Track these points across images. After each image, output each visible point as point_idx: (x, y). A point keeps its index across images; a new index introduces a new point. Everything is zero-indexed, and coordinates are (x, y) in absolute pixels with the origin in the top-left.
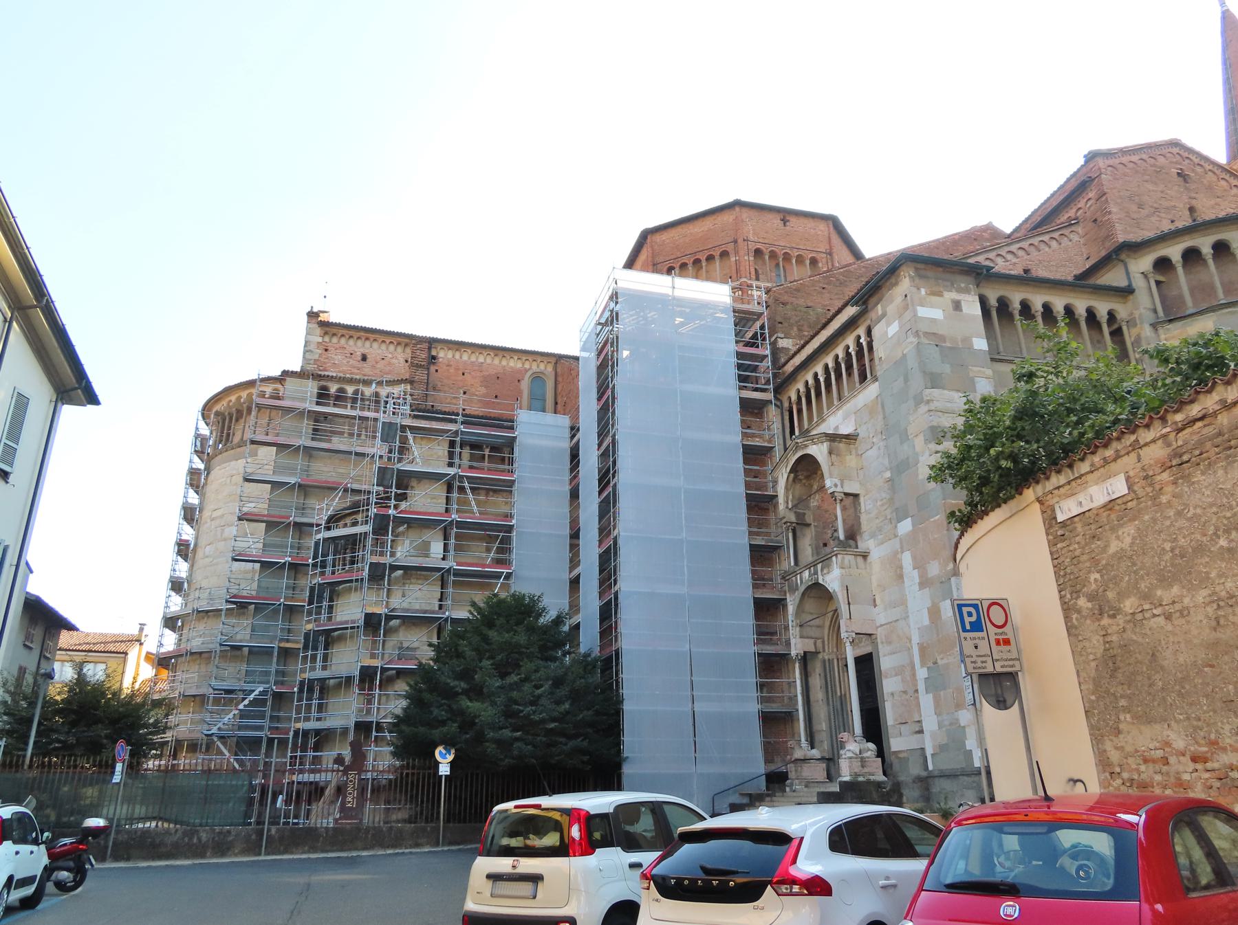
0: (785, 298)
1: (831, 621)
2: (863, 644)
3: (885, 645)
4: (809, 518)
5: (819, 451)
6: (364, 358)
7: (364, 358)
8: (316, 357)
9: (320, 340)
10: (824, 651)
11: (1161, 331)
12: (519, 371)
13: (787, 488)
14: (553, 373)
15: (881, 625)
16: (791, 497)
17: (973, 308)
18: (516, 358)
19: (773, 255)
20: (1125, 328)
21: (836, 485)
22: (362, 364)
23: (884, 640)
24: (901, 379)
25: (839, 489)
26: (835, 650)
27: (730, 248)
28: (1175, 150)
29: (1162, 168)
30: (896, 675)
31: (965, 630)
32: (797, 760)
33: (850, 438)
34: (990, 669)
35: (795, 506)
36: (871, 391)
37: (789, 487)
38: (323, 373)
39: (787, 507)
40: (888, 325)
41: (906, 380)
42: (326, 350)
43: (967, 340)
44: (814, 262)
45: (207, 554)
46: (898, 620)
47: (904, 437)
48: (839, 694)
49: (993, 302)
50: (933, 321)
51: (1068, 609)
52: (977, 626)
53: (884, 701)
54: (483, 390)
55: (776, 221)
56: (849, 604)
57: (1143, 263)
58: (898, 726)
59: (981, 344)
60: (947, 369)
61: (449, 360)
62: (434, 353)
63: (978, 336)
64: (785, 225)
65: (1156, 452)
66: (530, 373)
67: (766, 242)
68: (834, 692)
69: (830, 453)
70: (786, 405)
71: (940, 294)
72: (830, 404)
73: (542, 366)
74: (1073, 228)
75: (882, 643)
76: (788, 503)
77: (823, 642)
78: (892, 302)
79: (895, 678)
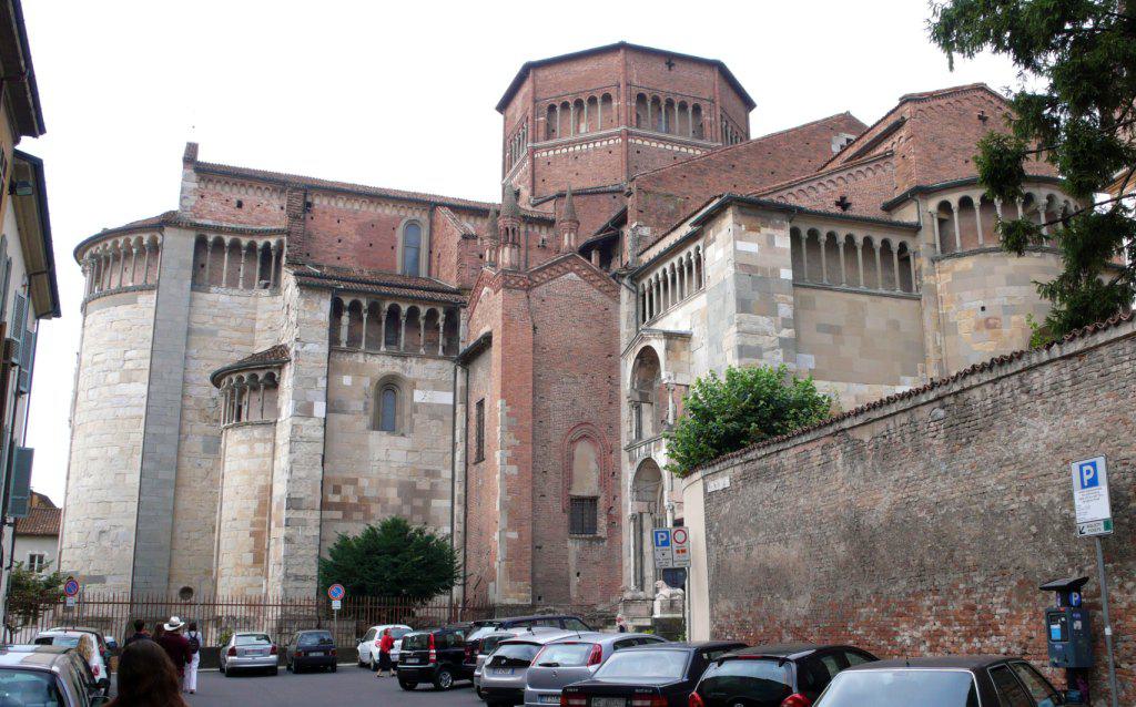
0: (648, 186)
5: (659, 346)
6: (240, 205)
7: (240, 205)
8: (193, 203)
9: (196, 185)
11: (936, 265)
12: (395, 218)
13: (633, 372)
14: (428, 221)
17: (783, 241)
18: (391, 205)
19: (656, 101)
20: (912, 258)
21: (669, 378)
22: (237, 211)
24: (722, 299)
25: (672, 381)
27: (613, 92)
28: (981, 93)
29: (965, 111)
31: (657, 545)
33: (685, 337)
34: (670, 566)
35: (640, 387)
36: (699, 302)
38: (198, 221)
40: (716, 249)
41: (725, 302)
42: (202, 197)
43: (776, 271)
44: (697, 109)
45: (91, 398)
47: (720, 349)
49: (804, 234)
50: (749, 254)
51: (708, 539)
52: (666, 543)
54: (358, 238)
55: (661, 66)
57: (932, 205)
59: (787, 274)
60: (756, 296)
61: (325, 207)
62: (309, 199)
63: (786, 267)
64: (670, 69)
65: (738, 470)
66: (405, 221)
67: (650, 86)
69: (667, 349)
70: (641, 291)
71: (757, 230)
72: (674, 302)
73: (417, 215)
74: (888, 160)
78: (721, 230)
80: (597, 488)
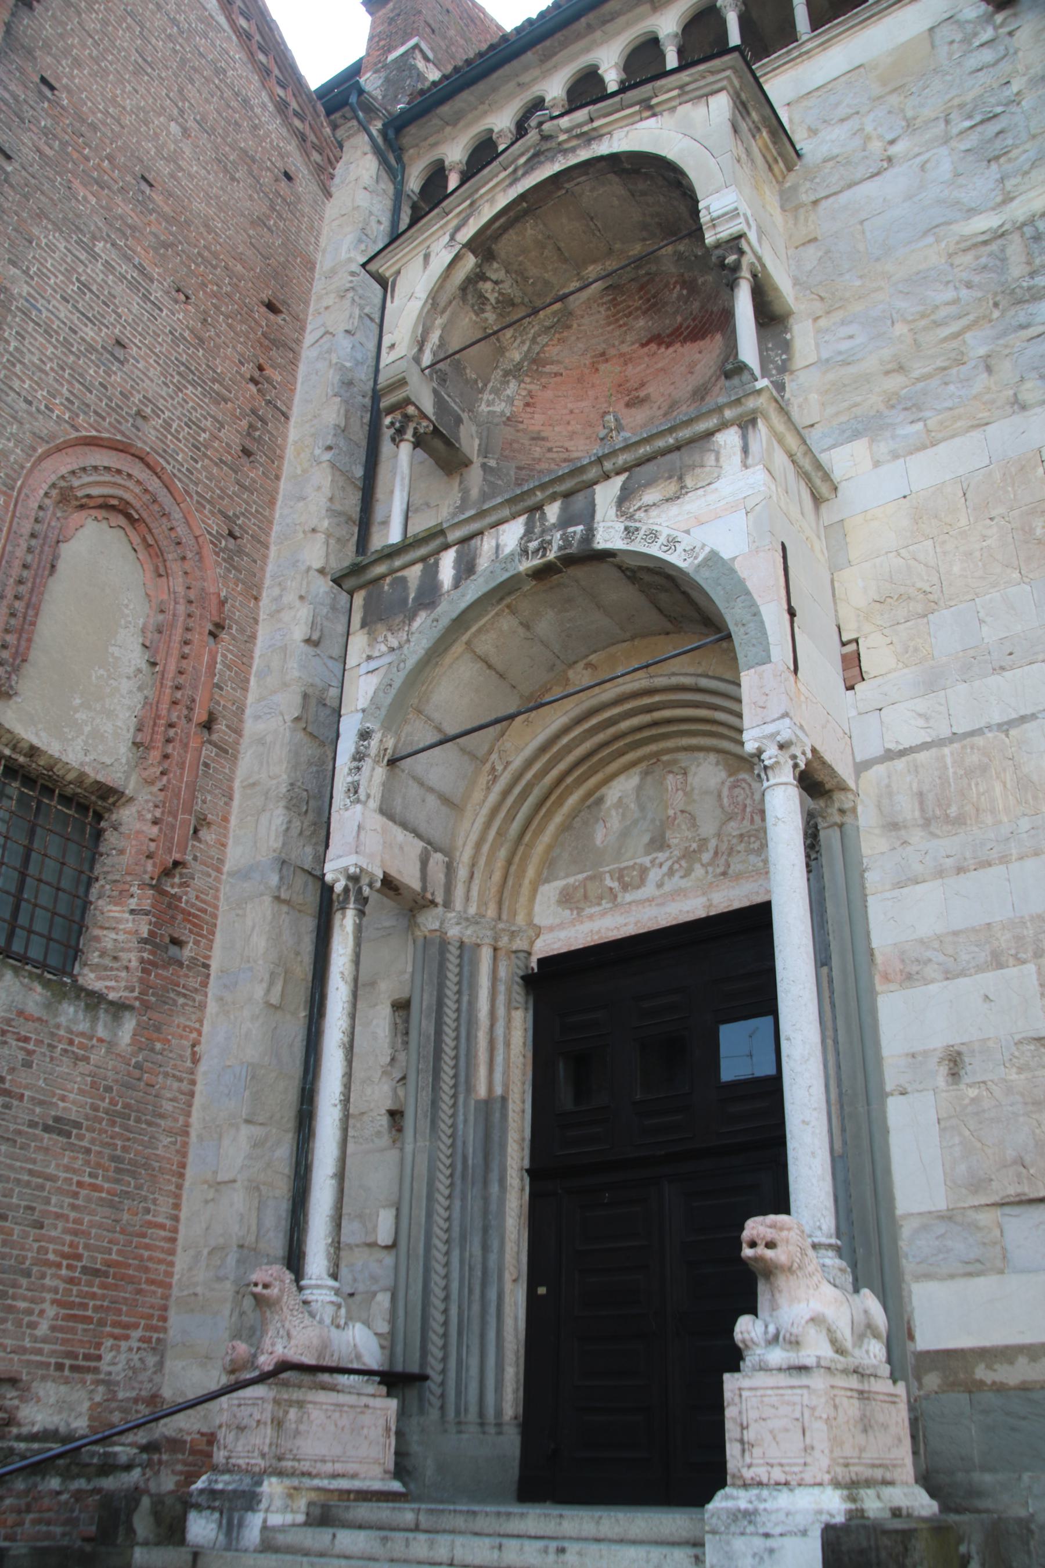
1: (506, 793)
2: (649, 890)
3: (917, 836)
4: (469, 440)
10: (447, 904)
13: (434, 302)
15: (890, 755)
16: (434, 338)
23: (907, 809)
26: (491, 912)
30: (997, 962)
32: (284, 1366)
37: (443, 301)
39: (417, 360)
46: (1023, 719)
48: (482, 1092)
53: (884, 1095)
56: (792, 613)
58: (985, 1218)
68: (470, 1088)
75: (893, 826)
76: (421, 350)
77: (450, 869)
79: (990, 979)
80: (123, 750)
